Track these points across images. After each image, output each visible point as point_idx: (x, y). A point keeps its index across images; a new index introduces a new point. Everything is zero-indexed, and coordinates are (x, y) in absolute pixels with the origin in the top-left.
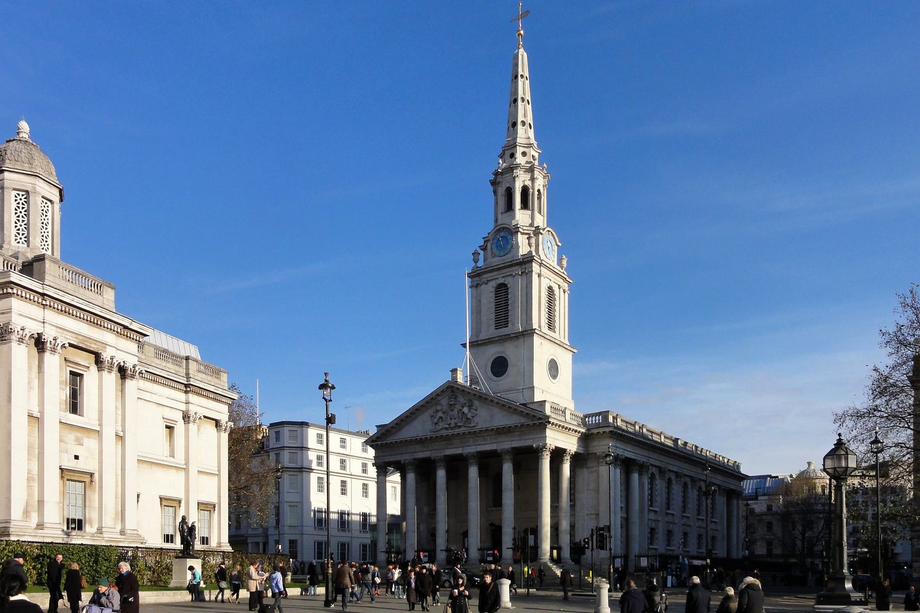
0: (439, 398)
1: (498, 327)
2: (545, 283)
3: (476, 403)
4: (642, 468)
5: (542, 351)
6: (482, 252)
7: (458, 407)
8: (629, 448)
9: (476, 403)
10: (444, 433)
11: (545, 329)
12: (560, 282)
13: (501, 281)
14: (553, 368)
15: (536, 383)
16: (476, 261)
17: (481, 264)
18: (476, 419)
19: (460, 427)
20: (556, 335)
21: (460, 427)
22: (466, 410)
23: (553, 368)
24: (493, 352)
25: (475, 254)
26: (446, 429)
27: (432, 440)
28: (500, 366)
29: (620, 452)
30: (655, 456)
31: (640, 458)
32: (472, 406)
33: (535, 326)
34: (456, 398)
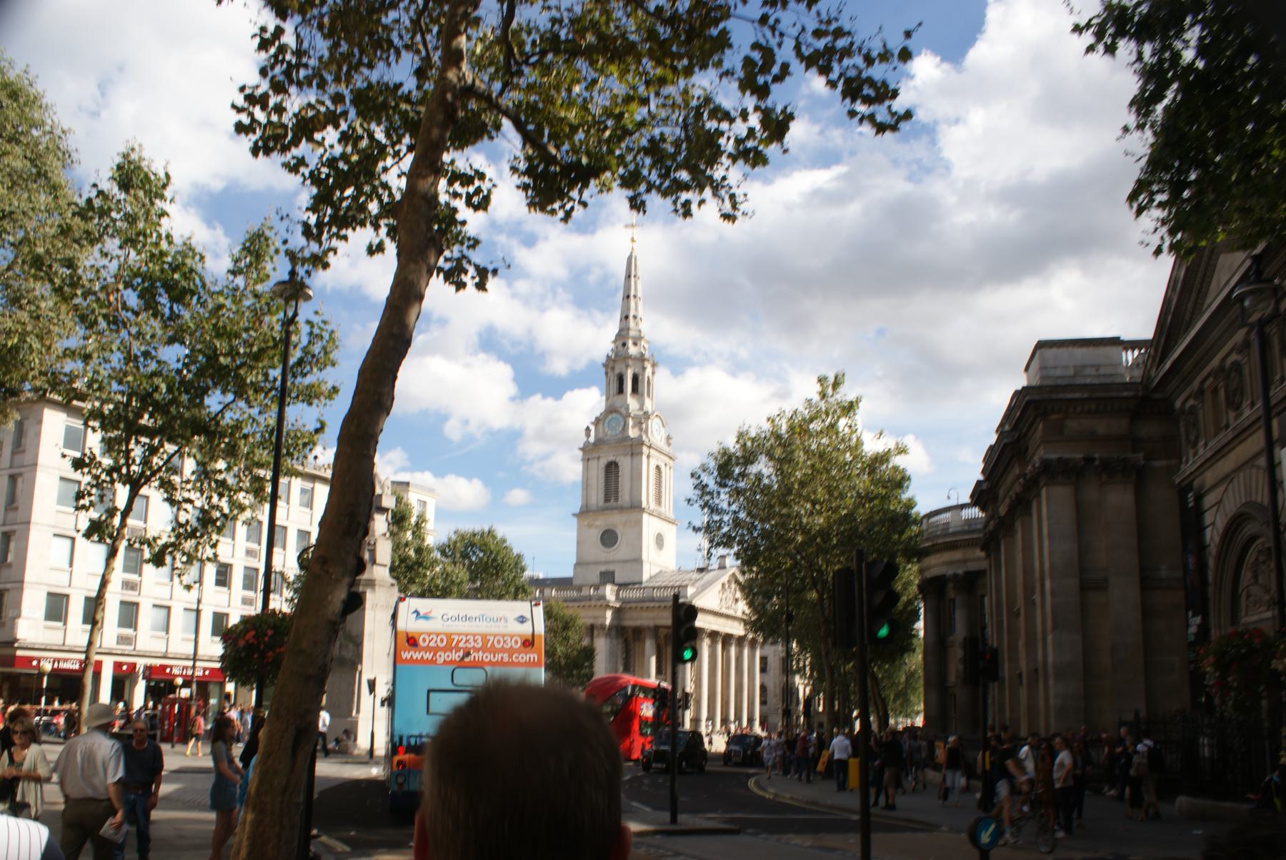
1: (607, 500)
2: (653, 462)
5: (650, 526)
6: (592, 428)
11: (653, 506)
12: (667, 459)
13: (611, 458)
14: (660, 540)
15: (644, 557)
16: (588, 435)
17: (592, 439)
20: (662, 509)
23: (660, 540)
24: (602, 522)
25: (588, 429)
28: (609, 538)
33: (644, 505)
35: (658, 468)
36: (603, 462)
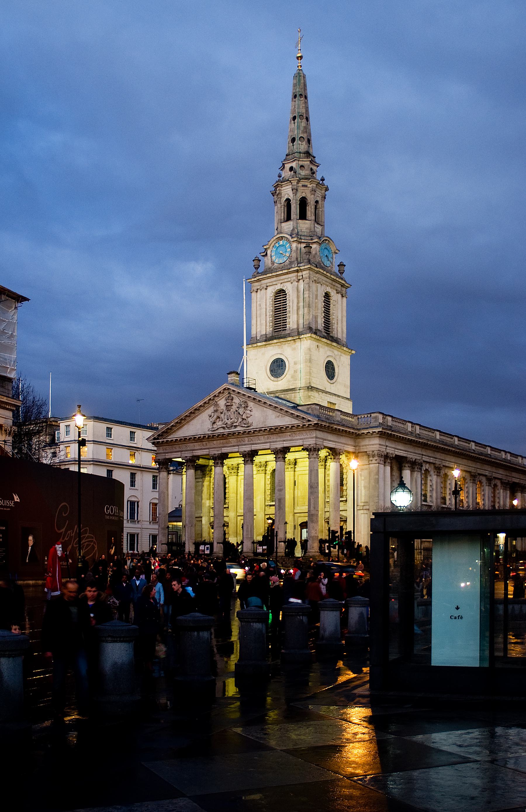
0: (216, 399)
3: (251, 404)
4: (414, 465)
7: (234, 407)
8: (400, 446)
9: (251, 404)
10: (221, 431)
13: (279, 287)
18: (250, 420)
19: (236, 427)
21: (236, 427)
22: (241, 411)
26: (224, 428)
27: (210, 438)
28: (278, 367)
29: (390, 451)
30: (429, 453)
31: (412, 456)
32: (247, 407)
34: (232, 400)
35: (327, 296)
36: (271, 292)
